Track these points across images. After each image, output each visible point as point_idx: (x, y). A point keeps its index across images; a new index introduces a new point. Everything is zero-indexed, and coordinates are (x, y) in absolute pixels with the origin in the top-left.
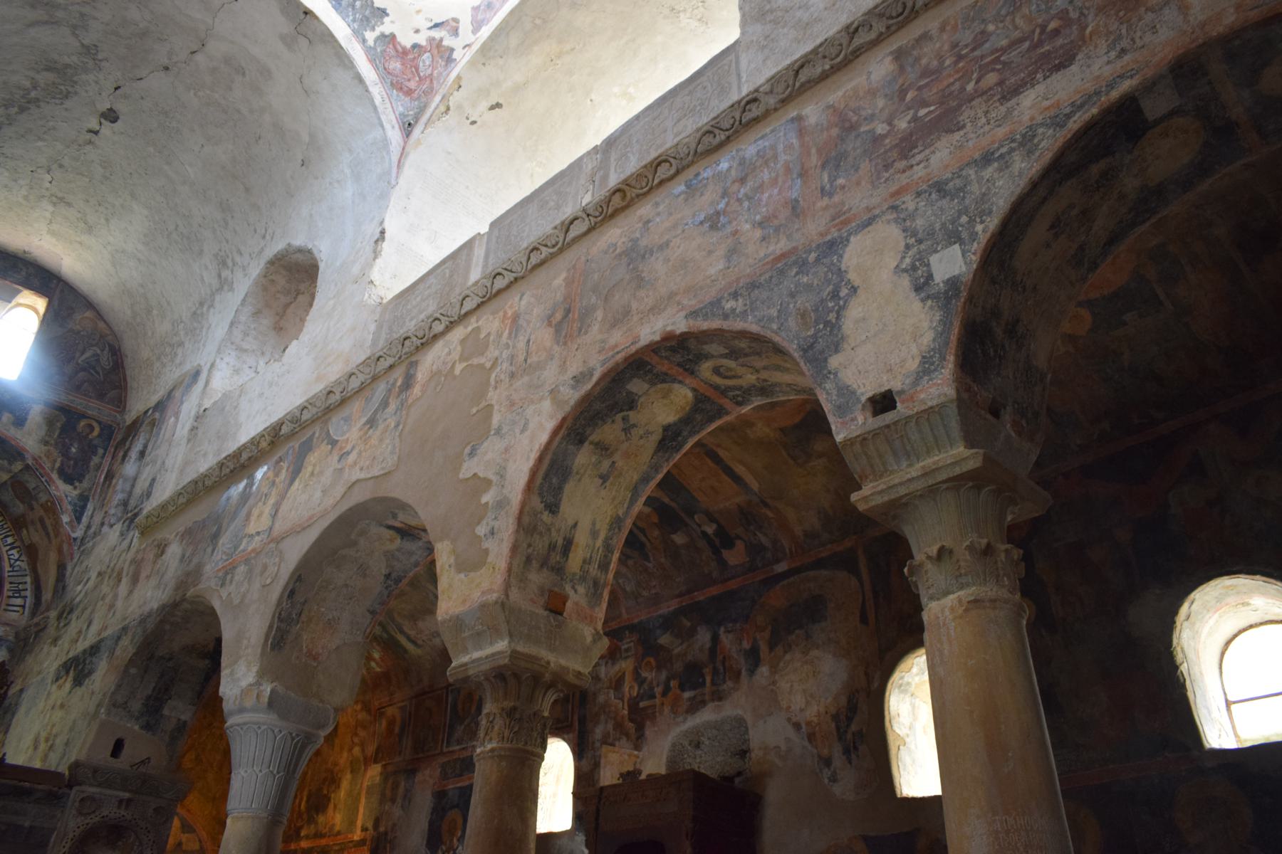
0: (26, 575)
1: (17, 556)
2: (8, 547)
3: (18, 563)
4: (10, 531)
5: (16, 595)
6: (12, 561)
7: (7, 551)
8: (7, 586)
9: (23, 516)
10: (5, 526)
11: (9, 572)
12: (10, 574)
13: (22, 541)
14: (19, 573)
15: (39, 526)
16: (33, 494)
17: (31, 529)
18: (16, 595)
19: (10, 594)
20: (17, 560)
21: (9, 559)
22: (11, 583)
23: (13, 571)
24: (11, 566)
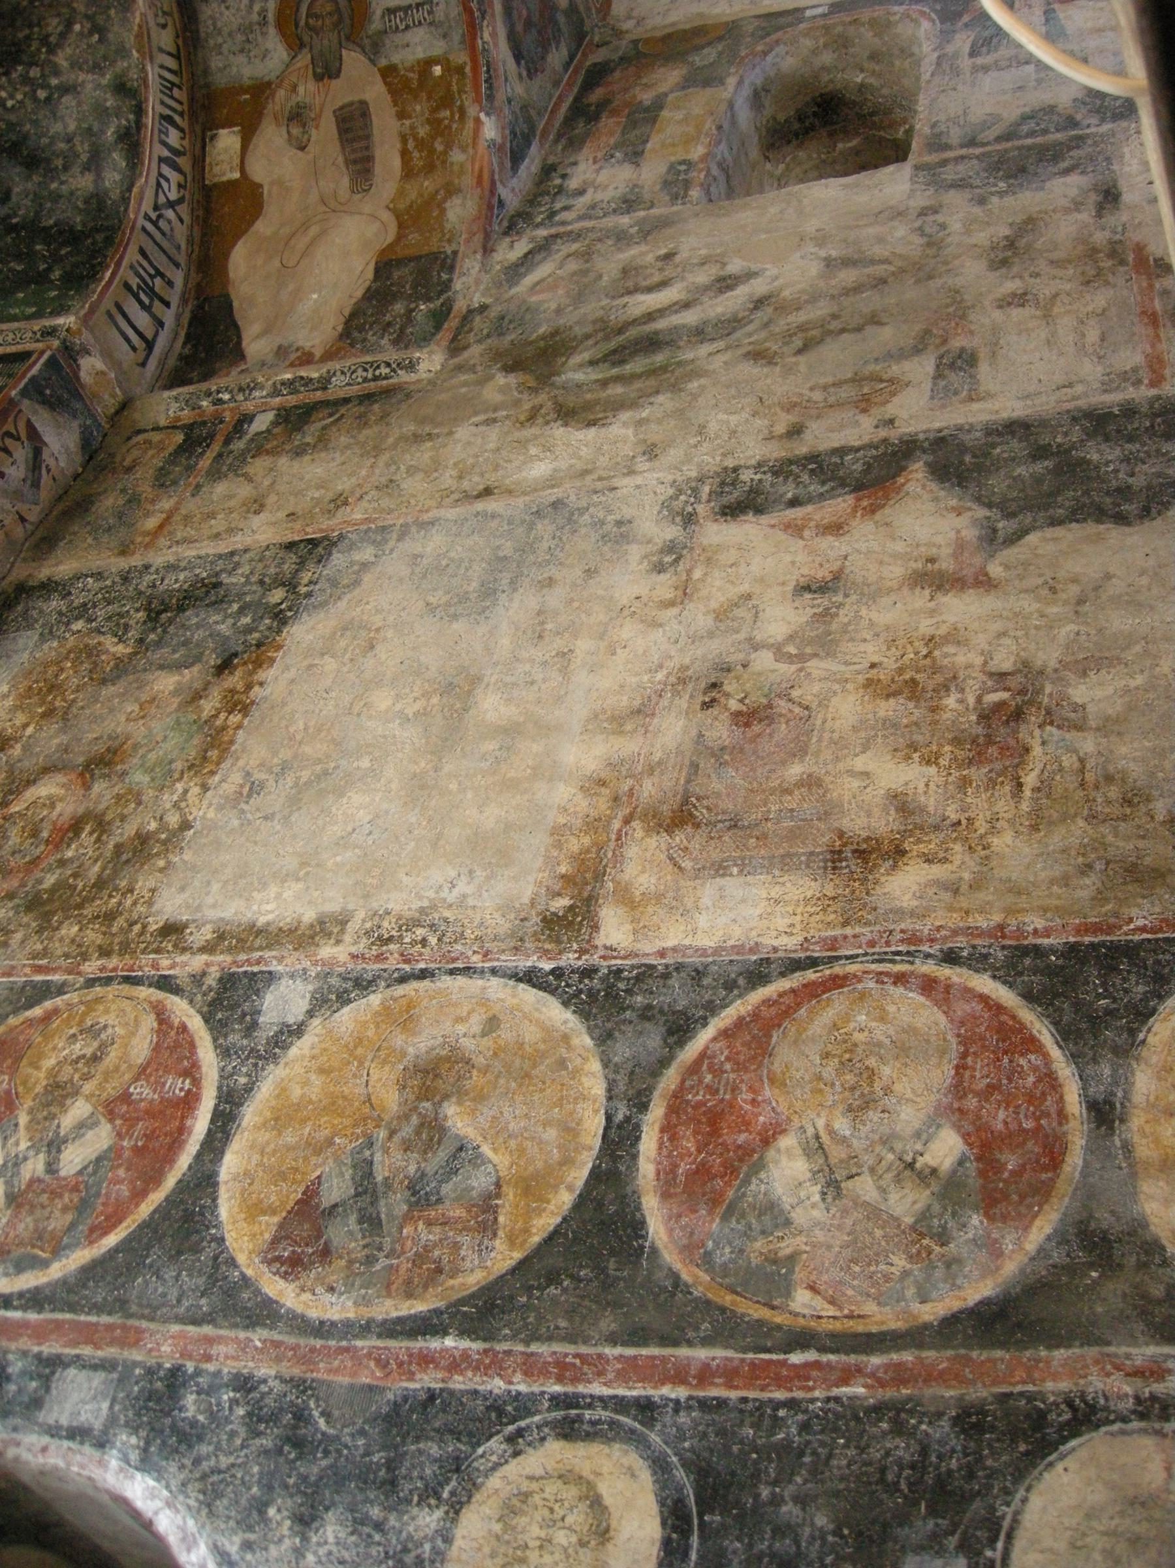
0: (177, 265)
1: (173, 196)
2: (166, 153)
3: (170, 214)
4: (181, 114)
5: (143, 296)
6: (162, 200)
7: (161, 160)
8: (132, 255)
9: (261, 90)
10: (176, 92)
11: (147, 217)
12: (150, 227)
13: (200, 161)
14: (165, 244)
15: (325, 132)
16: (376, 25)
17: (271, 136)
18: (143, 296)
19: (134, 282)
20: (171, 205)
21: (159, 185)
22: (142, 252)
23: (155, 223)
24: (156, 208)
